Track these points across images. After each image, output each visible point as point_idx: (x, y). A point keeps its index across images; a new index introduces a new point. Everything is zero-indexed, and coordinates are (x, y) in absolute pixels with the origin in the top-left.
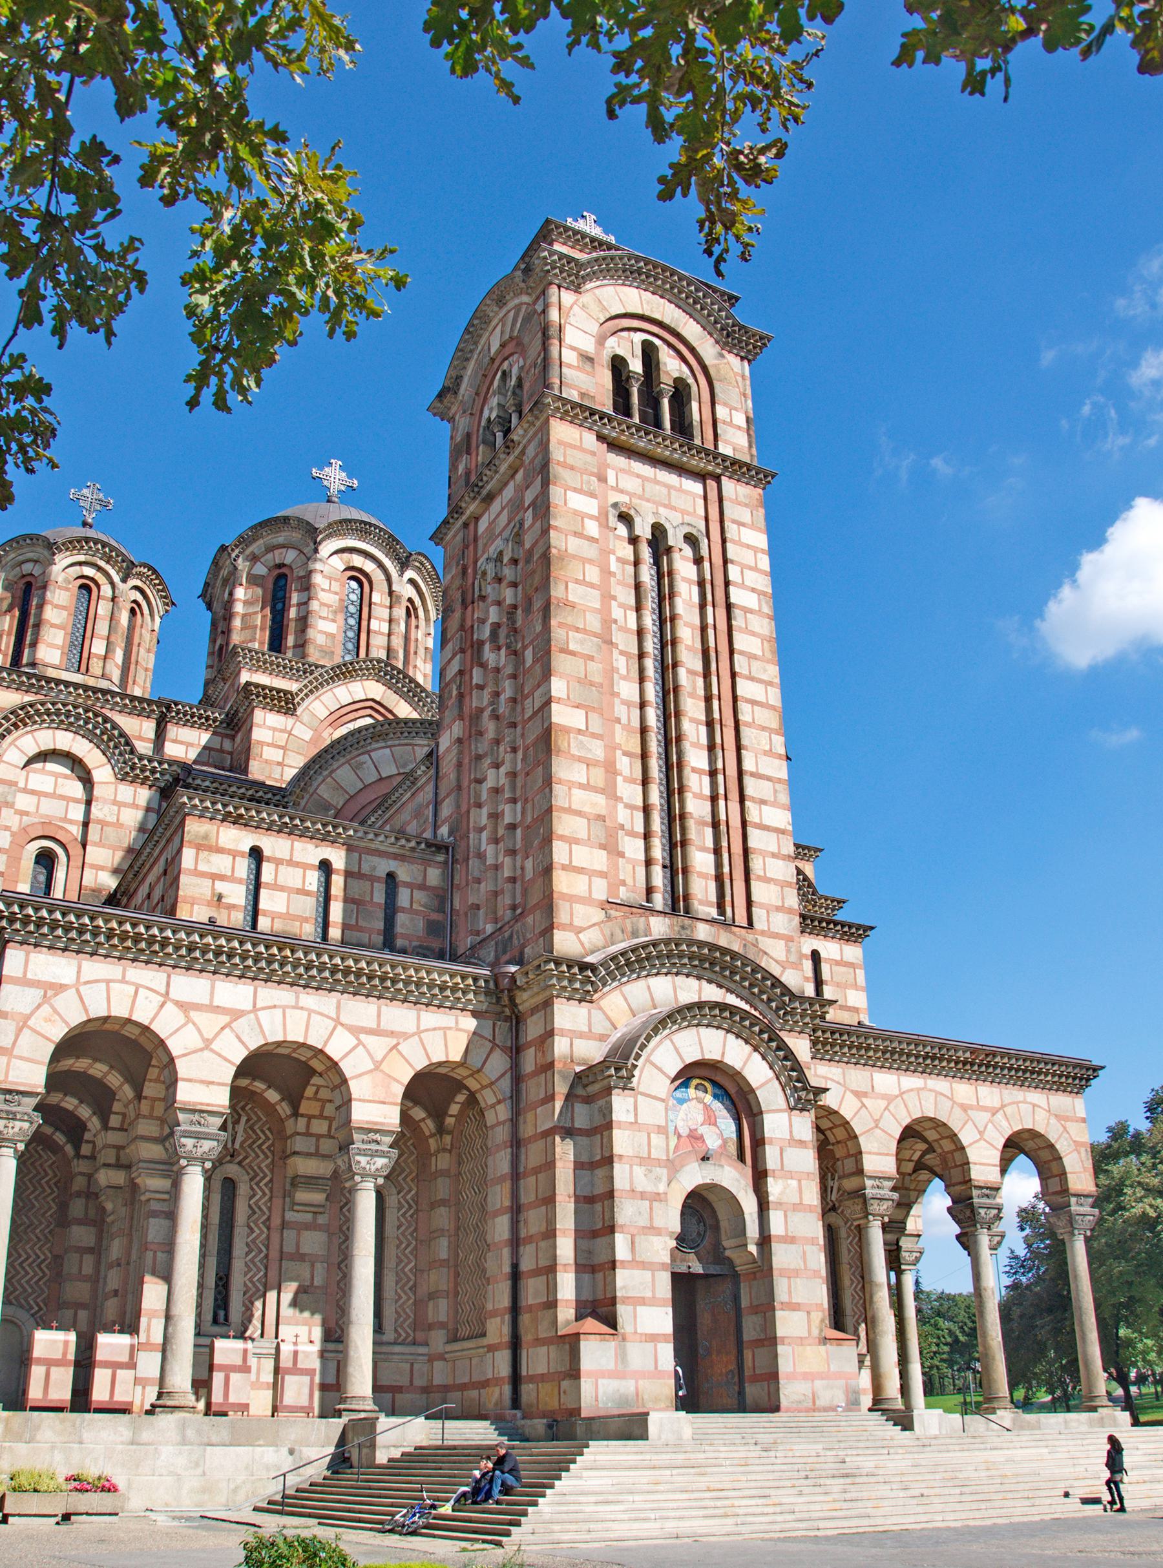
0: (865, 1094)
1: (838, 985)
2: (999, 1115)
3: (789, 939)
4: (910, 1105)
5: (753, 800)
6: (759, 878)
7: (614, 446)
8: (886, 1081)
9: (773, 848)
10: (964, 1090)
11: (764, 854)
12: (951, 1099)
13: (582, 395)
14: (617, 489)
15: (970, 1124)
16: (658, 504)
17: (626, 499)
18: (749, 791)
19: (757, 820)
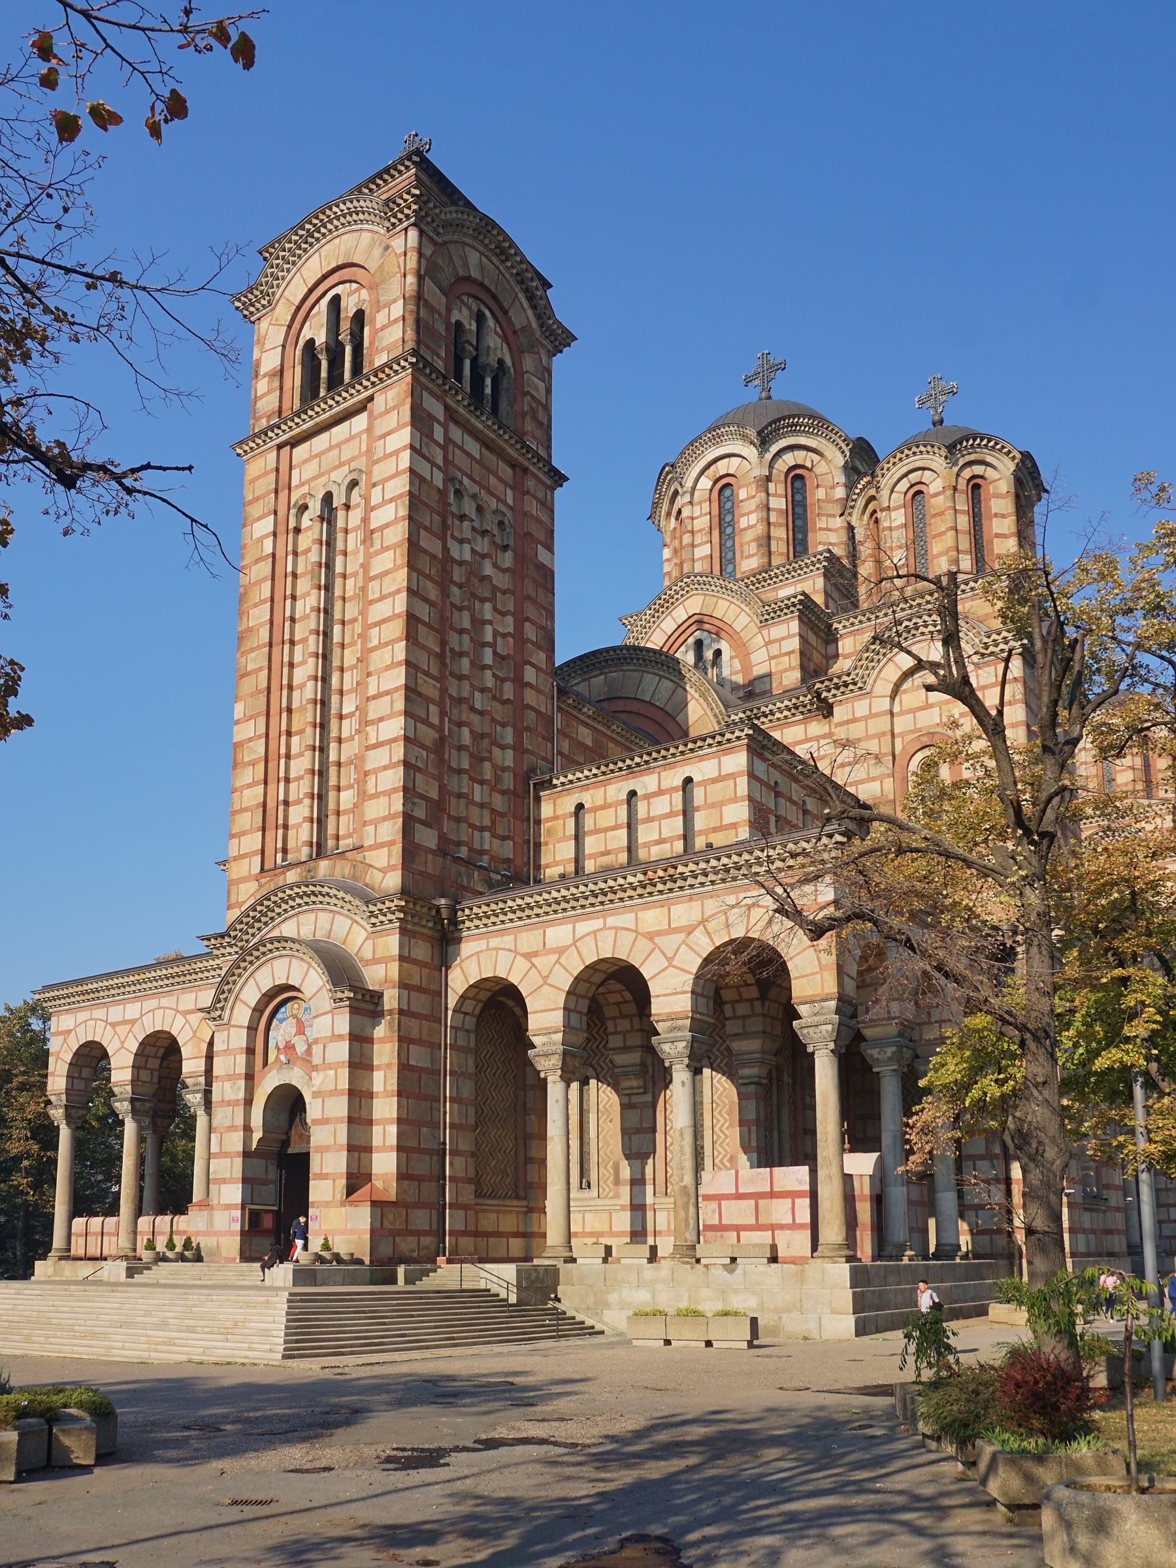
0: (536, 954)
1: (713, 806)
2: (697, 933)
3: (391, 843)
4: (584, 951)
5: (373, 722)
6: (372, 797)
7: (294, 443)
8: (558, 934)
9: (386, 762)
10: (652, 918)
11: (376, 771)
12: (635, 931)
13: (269, 418)
14: (302, 484)
15: (657, 951)
16: (329, 472)
17: (305, 489)
18: (371, 716)
19: (374, 741)
